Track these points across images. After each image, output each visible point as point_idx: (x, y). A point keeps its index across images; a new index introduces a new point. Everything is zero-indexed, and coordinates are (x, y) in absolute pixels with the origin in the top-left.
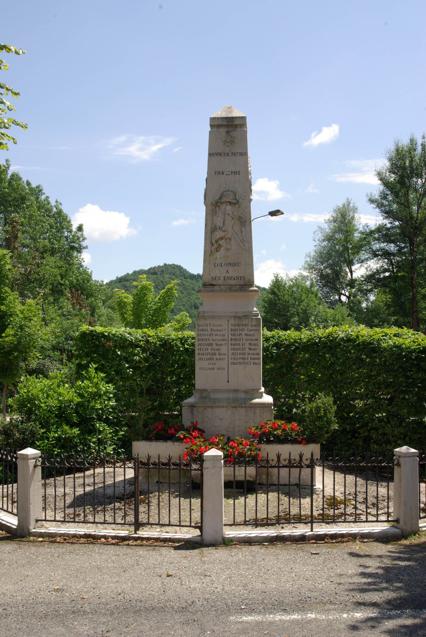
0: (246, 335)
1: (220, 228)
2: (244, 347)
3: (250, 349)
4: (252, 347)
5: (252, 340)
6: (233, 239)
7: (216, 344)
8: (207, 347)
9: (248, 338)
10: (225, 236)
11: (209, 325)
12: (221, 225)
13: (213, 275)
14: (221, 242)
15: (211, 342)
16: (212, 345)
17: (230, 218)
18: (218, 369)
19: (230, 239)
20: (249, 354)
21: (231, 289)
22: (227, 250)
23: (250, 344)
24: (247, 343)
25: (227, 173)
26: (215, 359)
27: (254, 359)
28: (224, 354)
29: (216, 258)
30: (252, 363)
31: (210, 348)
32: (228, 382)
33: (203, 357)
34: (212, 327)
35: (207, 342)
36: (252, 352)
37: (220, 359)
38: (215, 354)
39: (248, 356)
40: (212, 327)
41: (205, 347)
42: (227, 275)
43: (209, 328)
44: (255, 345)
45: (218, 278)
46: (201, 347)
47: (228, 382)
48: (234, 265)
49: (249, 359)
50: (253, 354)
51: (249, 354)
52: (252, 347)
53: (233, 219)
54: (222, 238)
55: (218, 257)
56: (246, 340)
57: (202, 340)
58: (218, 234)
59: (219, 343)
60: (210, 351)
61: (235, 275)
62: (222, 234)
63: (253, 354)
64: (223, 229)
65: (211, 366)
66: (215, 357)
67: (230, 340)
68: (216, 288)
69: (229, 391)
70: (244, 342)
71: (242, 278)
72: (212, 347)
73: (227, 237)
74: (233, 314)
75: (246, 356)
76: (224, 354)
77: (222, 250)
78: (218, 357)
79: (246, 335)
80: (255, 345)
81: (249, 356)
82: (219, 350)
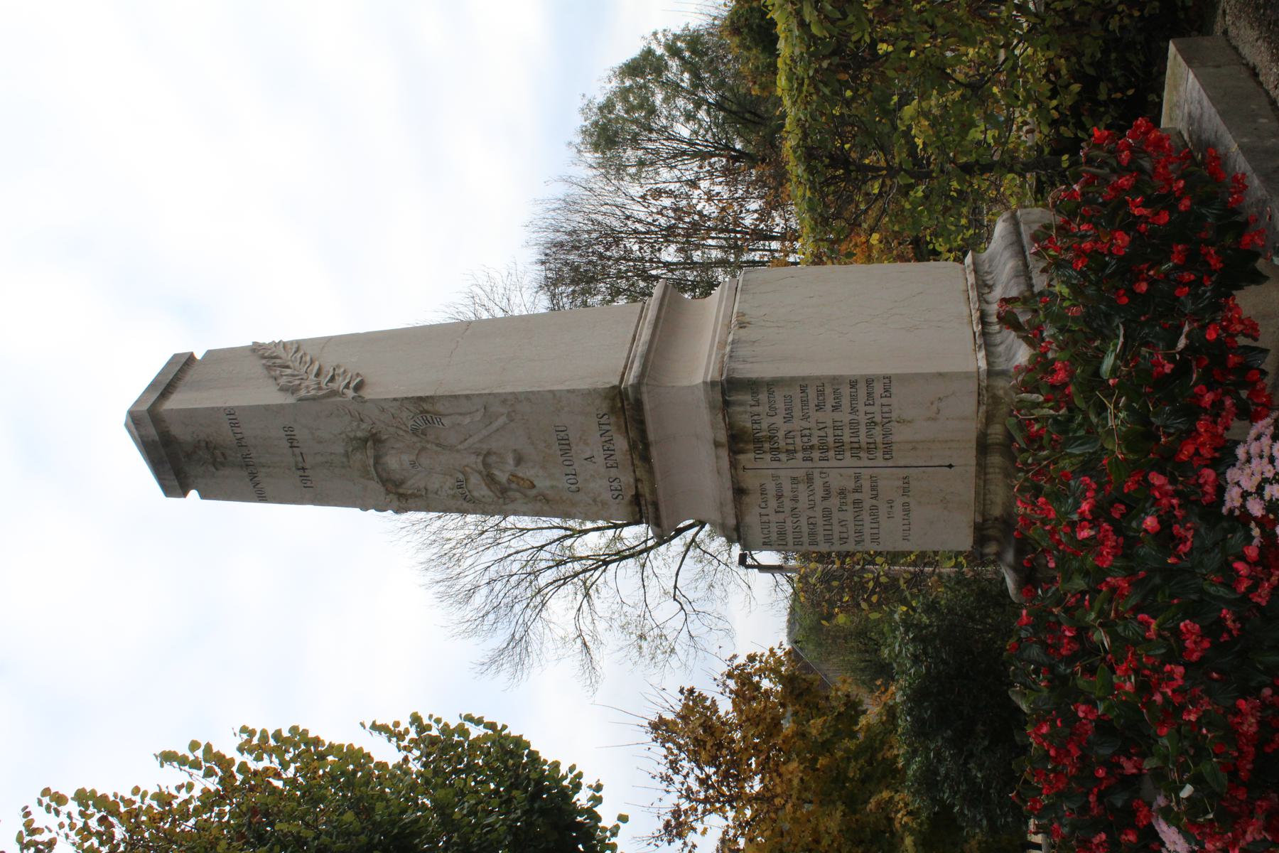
0: (788, 419)
1: (460, 487)
2: (830, 423)
3: (836, 408)
4: (830, 401)
5: (805, 403)
6: (485, 447)
7: (824, 499)
8: (835, 521)
9: (797, 412)
10: (480, 473)
11: (765, 519)
12: (450, 482)
13: (607, 496)
14: (502, 477)
15: (818, 513)
16: (827, 514)
17: (425, 461)
18: (906, 492)
19: (489, 453)
20: (854, 410)
21: (641, 449)
22: (519, 460)
23: (819, 407)
24: (815, 416)
25: (300, 459)
26: (874, 502)
27: (869, 395)
28: (857, 478)
29: (552, 487)
30: (885, 401)
31: (836, 516)
32: (950, 466)
33: (867, 531)
34: (770, 511)
35: (820, 522)
36: (845, 402)
37: (873, 488)
38: (857, 503)
39: (861, 414)
40: (770, 511)
41: (836, 528)
42: (600, 459)
43: (774, 518)
44: (821, 393)
45: (615, 484)
46: (836, 536)
47: (950, 466)
48: (565, 445)
49: (869, 409)
50: (853, 398)
51: (854, 410)
52: (830, 401)
53: (423, 449)
54: (490, 479)
55: (548, 483)
56: (806, 417)
57: (812, 534)
58: (481, 490)
59: (819, 492)
60: (849, 516)
61: (595, 437)
62: (475, 480)
63: (853, 398)
64: (461, 477)
65: (898, 511)
66: (867, 503)
67: (809, 464)
68: (645, 489)
69: (982, 468)
70: (812, 424)
71: (603, 421)
72: (835, 510)
73: (481, 467)
74: (724, 453)
75: (863, 419)
76: (857, 478)
77: (526, 472)
78: (865, 496)
79: (788, 419)
80: (821, 393)
81: (862, 408)
82: (842, 493)
